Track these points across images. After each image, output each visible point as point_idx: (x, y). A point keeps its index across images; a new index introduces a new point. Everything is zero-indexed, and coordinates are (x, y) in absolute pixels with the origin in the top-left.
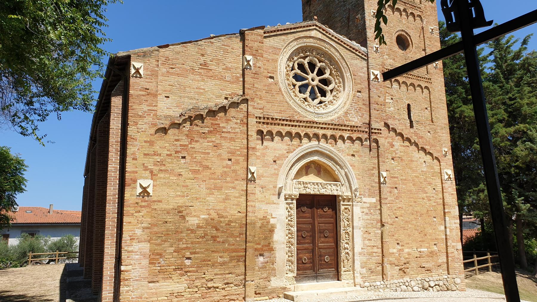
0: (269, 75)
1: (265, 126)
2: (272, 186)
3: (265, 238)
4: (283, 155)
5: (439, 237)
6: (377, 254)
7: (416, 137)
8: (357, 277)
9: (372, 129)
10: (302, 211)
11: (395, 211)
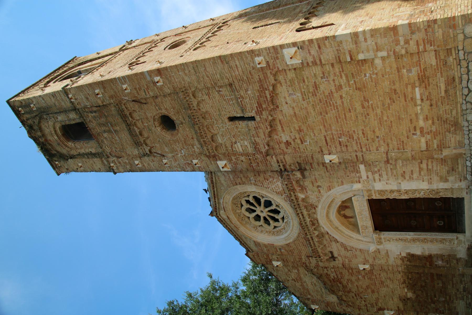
5: (394, 66)
6: (430, 163)
7: (264, 113)
8: (459, 186)
11: (370, 141)
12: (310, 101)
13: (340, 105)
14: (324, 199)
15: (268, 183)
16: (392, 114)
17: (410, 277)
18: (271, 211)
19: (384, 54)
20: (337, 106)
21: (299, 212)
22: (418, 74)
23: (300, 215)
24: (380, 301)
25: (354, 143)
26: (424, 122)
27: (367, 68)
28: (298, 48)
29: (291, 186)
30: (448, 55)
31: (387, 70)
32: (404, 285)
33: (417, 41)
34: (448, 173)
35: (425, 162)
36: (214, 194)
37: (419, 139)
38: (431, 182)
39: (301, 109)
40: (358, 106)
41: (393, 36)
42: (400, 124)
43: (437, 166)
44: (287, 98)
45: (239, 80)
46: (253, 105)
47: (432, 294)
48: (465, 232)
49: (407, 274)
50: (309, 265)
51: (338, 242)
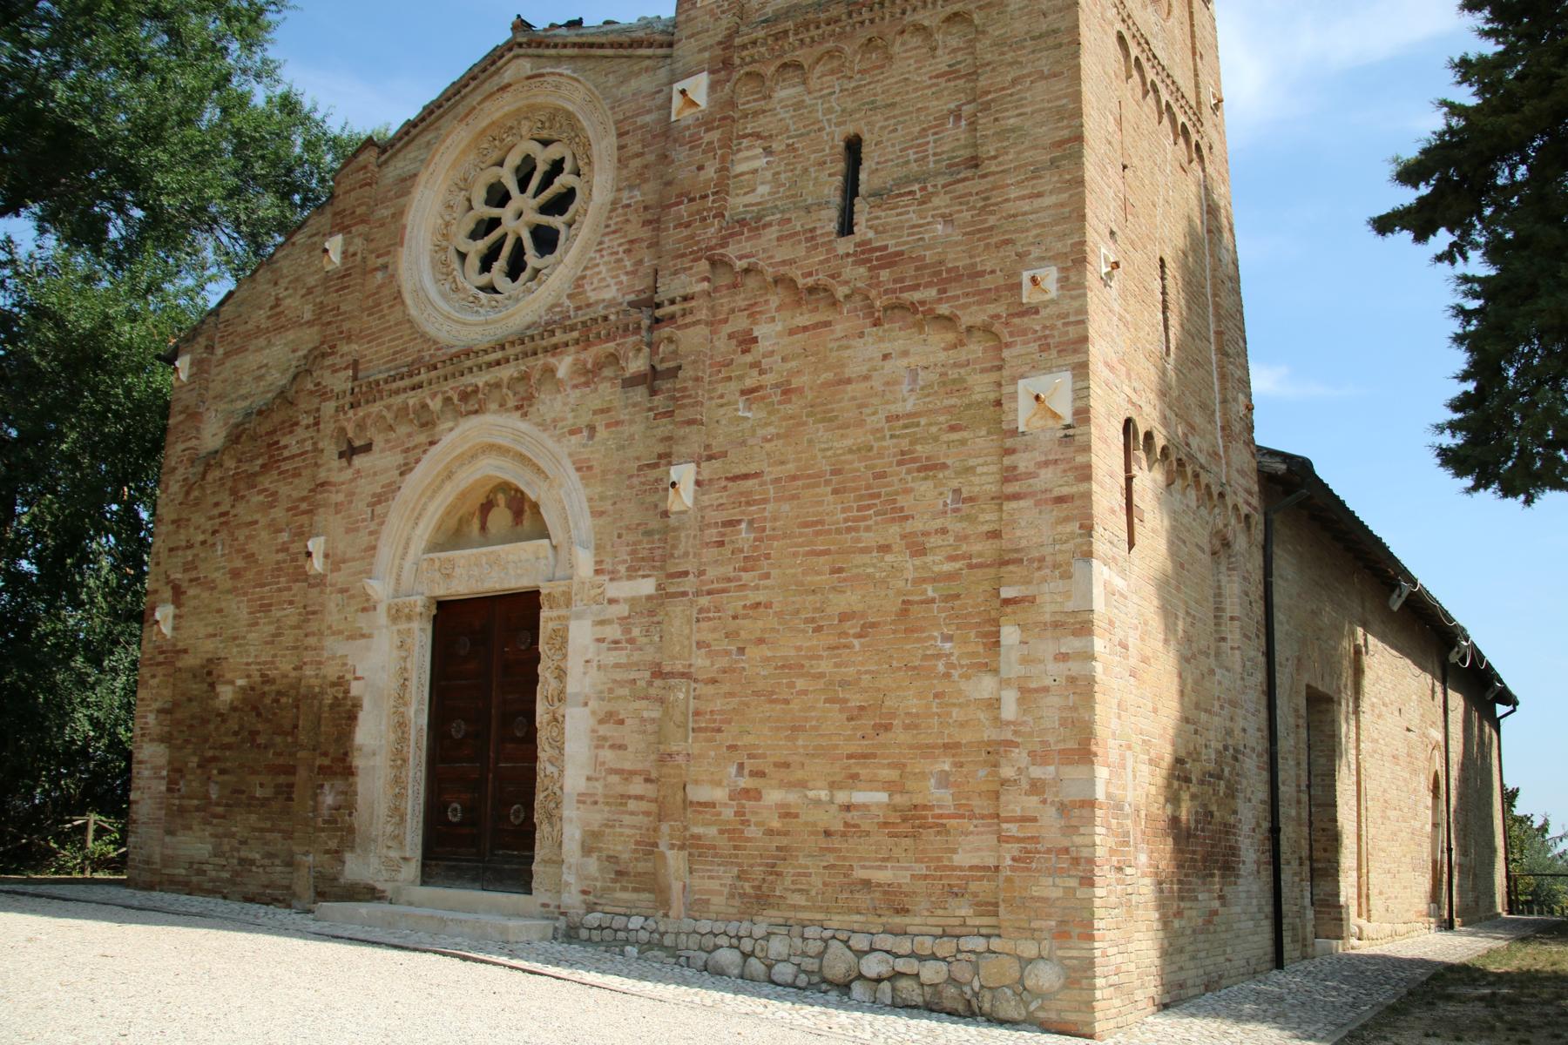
5: (966, 737)
6: (644, 806)
7: (862, 270)
8: (568, 884)
11: (733, 624)
12: (883, 438)
13: (859, 540)
14: (550, 443)
15: (617, 253)
16: (813, 708)
17: (283, 700)
18: (519, 247)
19: (1009, 710)
20: (856, 529)
21: (510, 351)
22: (931, 808)
23: (499, 355)
24: (206, 595)
25: (728, 570)
26: (779, 806)
27: (971, 648)
28: (1068, 427)
29: (598, 335)
30: (977, 904)
31: (955, 712)
32: (257, 678)
33: (1034, 820)
34: (609, 858)
35: (650, 790)
36: (591, 45)
37: (725, 782)
38: (584, 802)
39: (860, 406)
40: (850, 600)
41: (1061, 746)
42: (778, 729)
43: (634, 827)
44: (904, 362)
45: (987, 198)
46: (893, 237)
47: (229, 764)
48: (424, 883)
49: (293, 692)
50: (328, 367)
51: (402, 474)
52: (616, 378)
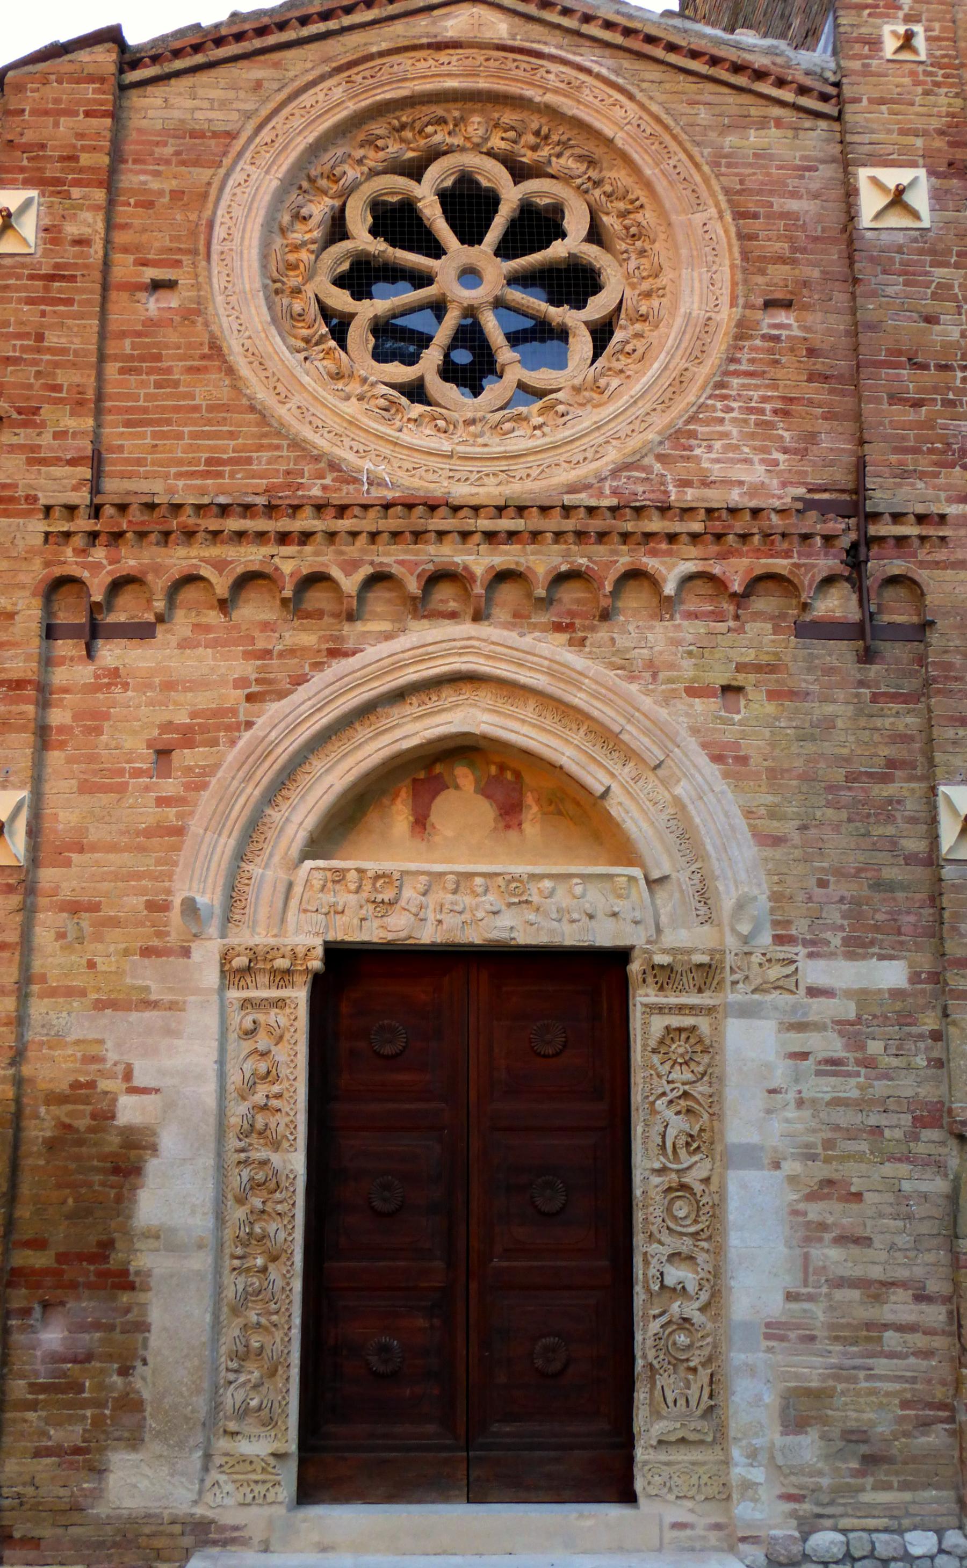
0: (150, 273)
1: (99, 554)
2: (138, 902)
3: (81, 1214)
4: (219, 713)
6: (918, 1340)
9: (875, 517)
10: (377, 1054)
14: (647, 703)
52: (783, 616)
